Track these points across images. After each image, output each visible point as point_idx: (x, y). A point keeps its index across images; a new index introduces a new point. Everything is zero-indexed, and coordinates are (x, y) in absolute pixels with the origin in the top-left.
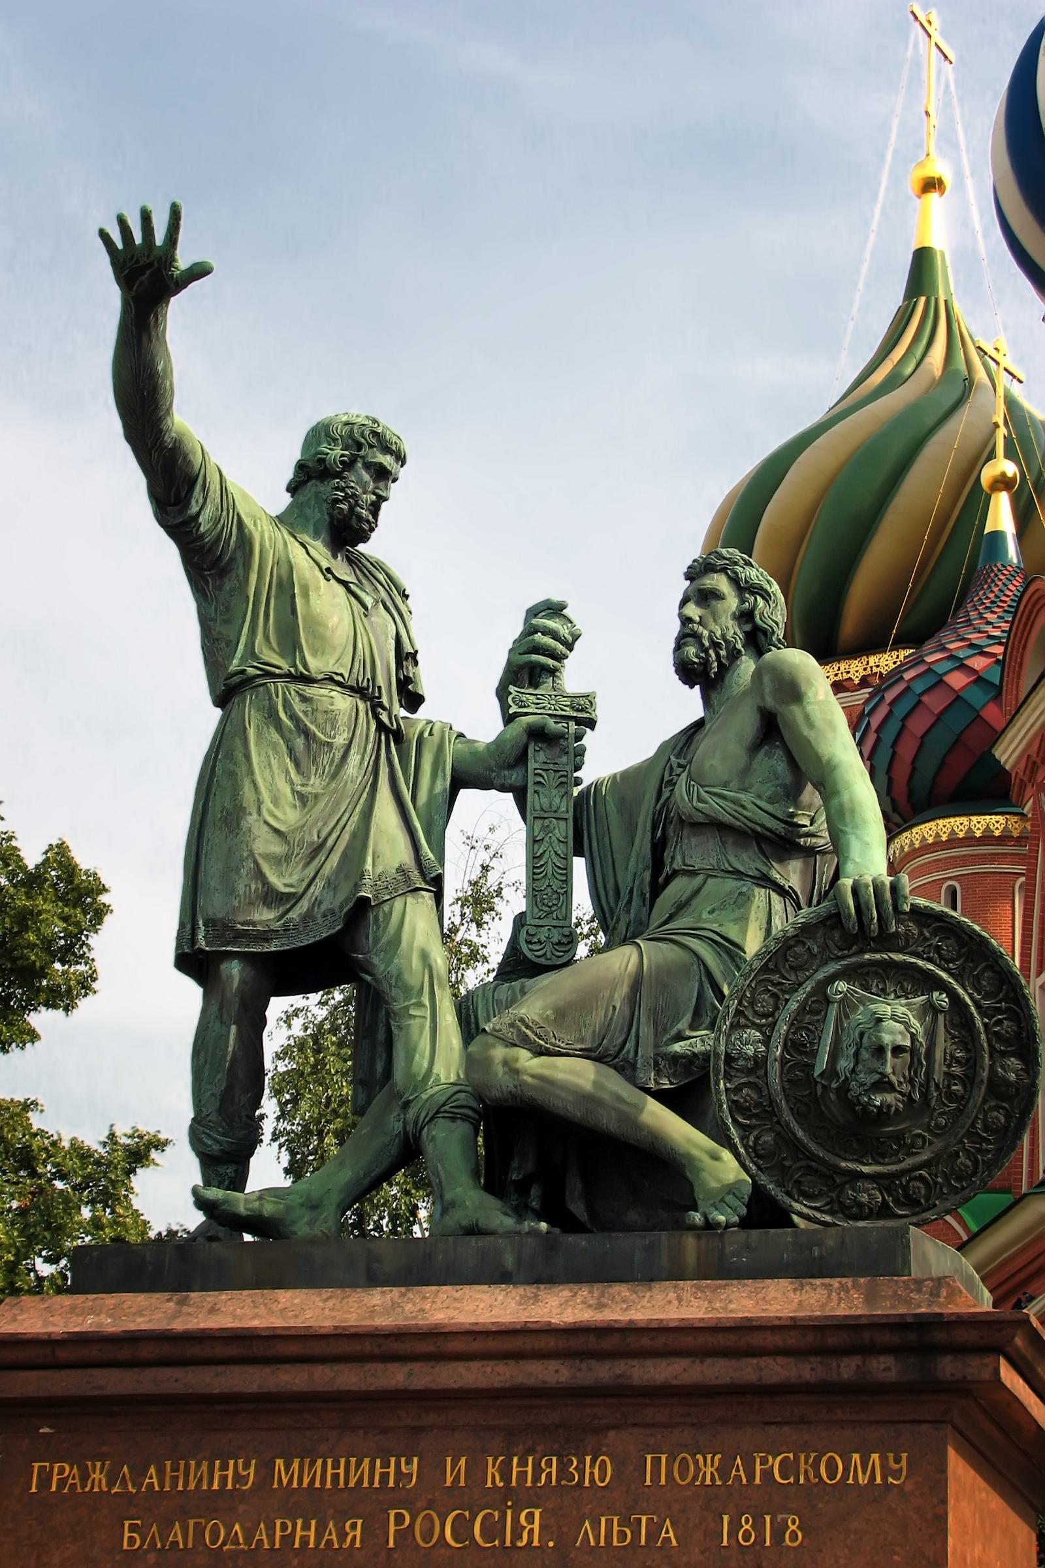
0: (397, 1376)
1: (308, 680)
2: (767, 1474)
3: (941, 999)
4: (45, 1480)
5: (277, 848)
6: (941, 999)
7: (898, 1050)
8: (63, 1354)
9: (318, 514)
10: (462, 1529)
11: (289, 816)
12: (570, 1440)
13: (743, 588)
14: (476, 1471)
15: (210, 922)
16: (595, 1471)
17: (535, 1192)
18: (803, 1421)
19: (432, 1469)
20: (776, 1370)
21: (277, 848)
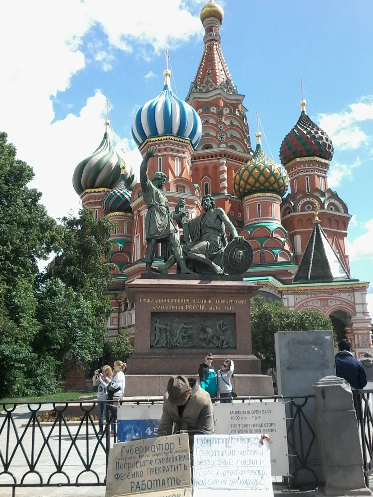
0: (189, 290)
1: (161, 206)
2: (230, 302)
3: (245, 251)
4: (142, 301)
5: (159, 226)
6: (245, 251)
7: (241, 256)
8: (147, 286)
9: (157, 184)
10: (195, 308)
11: (160, 222)
12: (208, 298)
13: (211, 199)
14: (196, 301)
15: (151, 234)
16: (211, 301)
17: (192, 269)
18: (234, 297)
19: (191, 301)
20: (233, 291)
21: (159, 226)
